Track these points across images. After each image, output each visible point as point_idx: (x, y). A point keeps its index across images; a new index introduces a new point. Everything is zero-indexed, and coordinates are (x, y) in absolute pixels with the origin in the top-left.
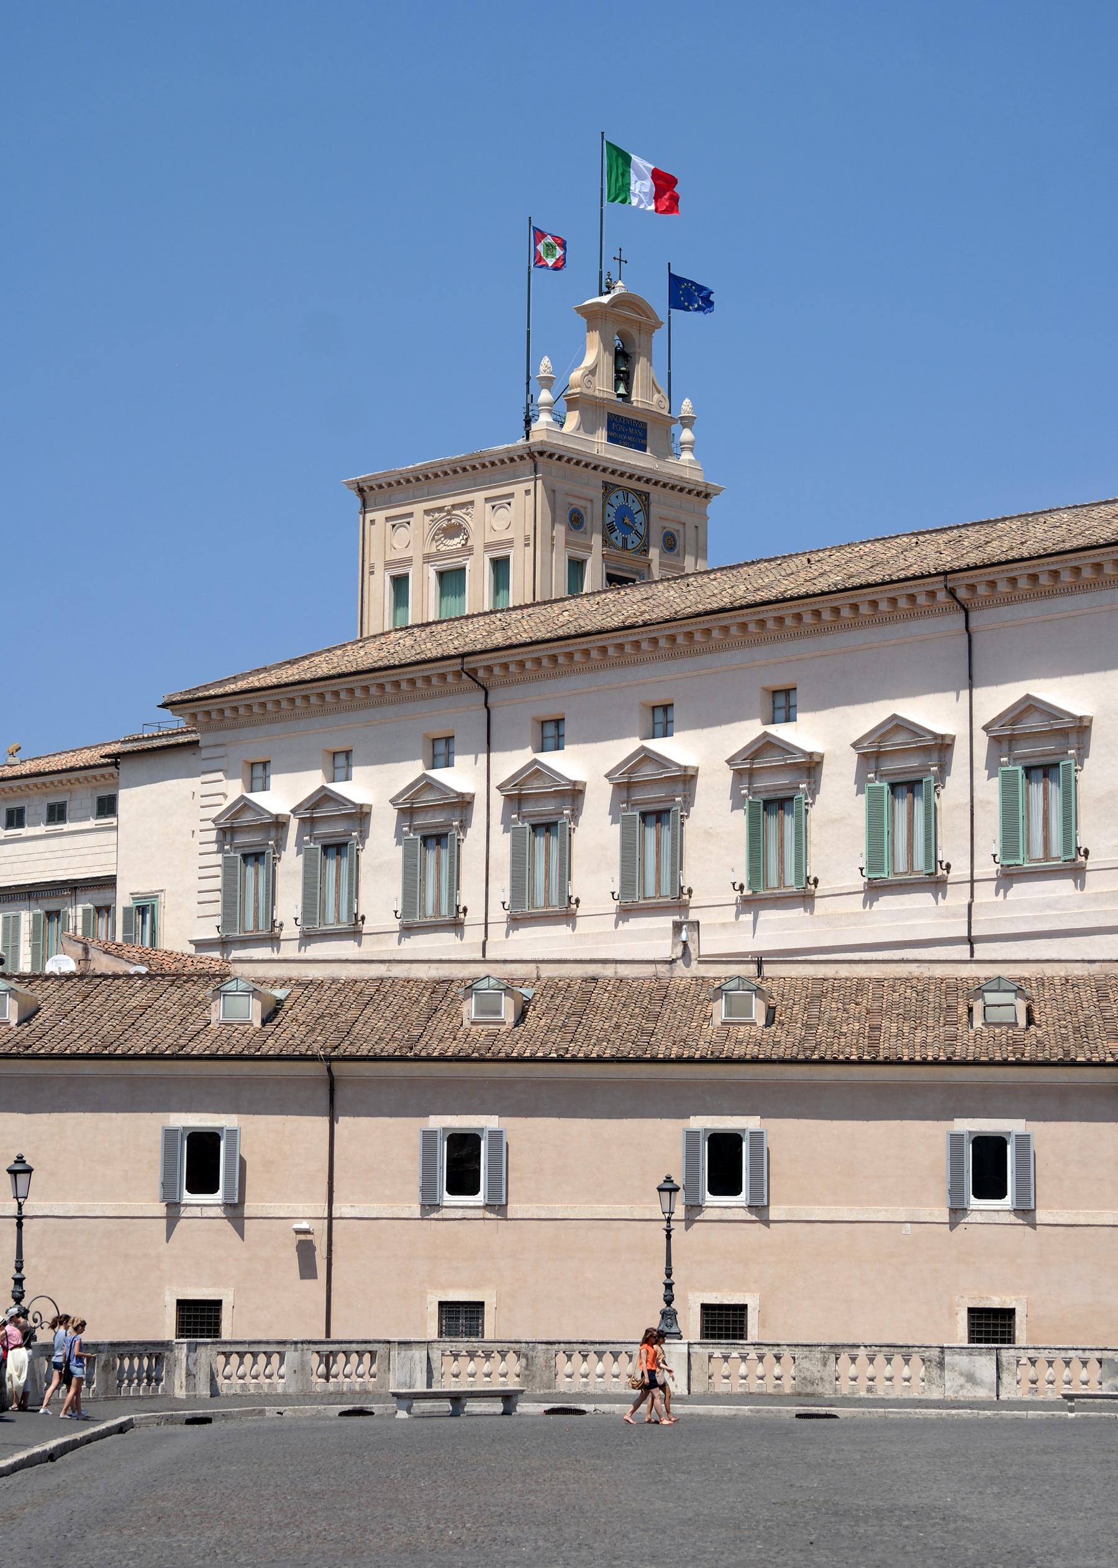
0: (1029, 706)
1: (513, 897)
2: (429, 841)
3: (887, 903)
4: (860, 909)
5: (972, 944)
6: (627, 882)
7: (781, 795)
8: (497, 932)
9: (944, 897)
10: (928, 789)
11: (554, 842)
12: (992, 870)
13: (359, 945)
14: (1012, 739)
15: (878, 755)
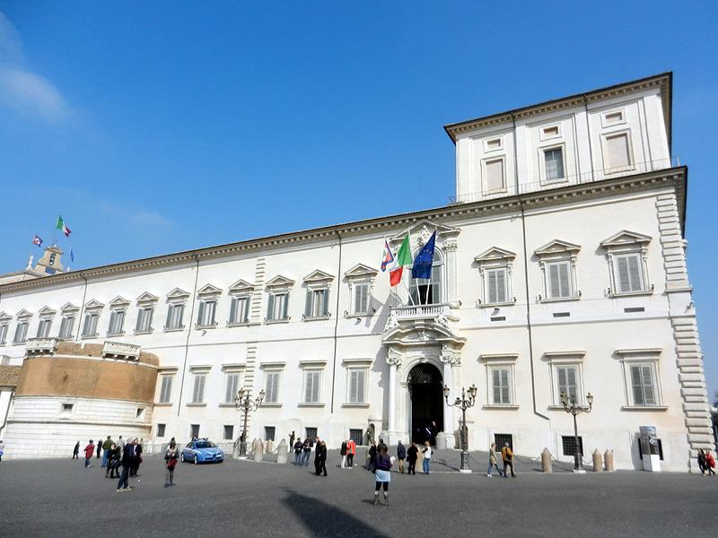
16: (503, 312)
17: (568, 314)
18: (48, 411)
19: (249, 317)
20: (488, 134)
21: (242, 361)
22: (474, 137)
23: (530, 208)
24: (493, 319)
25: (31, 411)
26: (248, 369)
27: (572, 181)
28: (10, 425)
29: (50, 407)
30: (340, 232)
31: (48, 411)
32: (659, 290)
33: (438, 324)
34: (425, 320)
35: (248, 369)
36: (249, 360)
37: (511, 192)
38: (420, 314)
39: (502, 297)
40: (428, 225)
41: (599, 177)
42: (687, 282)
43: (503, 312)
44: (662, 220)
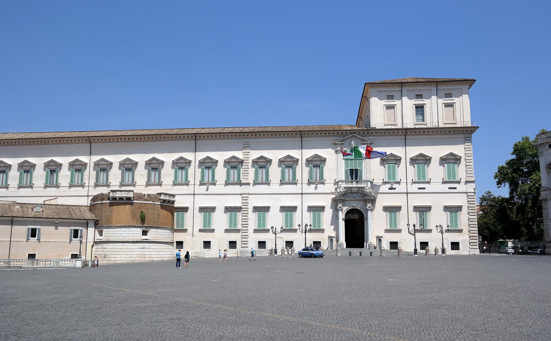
0: (26, 161)
1: (121, 181)
2: (76, 171)
3: (21, 190)
4: (17, 190)
5: (88, 197)
6: (72, 181)
7: (183, 167)
8: (197, 186)
9: (59, 189)
10: (57, 171)
11: (210, 171)
12: (93, 184)
13: (297, 186)
14: (257, 162)
15: (150, 164)
16: (394, 186)
17: (424, 188)
18: (135, 235)
19: (241, 179)
20: (388, 91)
21: (239, 204)
22: (379, 91)
23: (409, 135)
24: (389, 189)
25: (122, 235)
26: (243, 209)
27: (429, 125)
28: (100, 246)
29: (136, 233)
30: (303, 135)
31: (135, 235)
32: (463, 181)
33: (366, 191)
34: (358, 188)
35: (243, 209)
36: (243, 204)
37: (399, 126)
38: (354, 185)
39: (394, 179)
40: (355, 137)
41: (441, 125)
42: (474, 177)
43: (394, 186)
44: (466, 149)
